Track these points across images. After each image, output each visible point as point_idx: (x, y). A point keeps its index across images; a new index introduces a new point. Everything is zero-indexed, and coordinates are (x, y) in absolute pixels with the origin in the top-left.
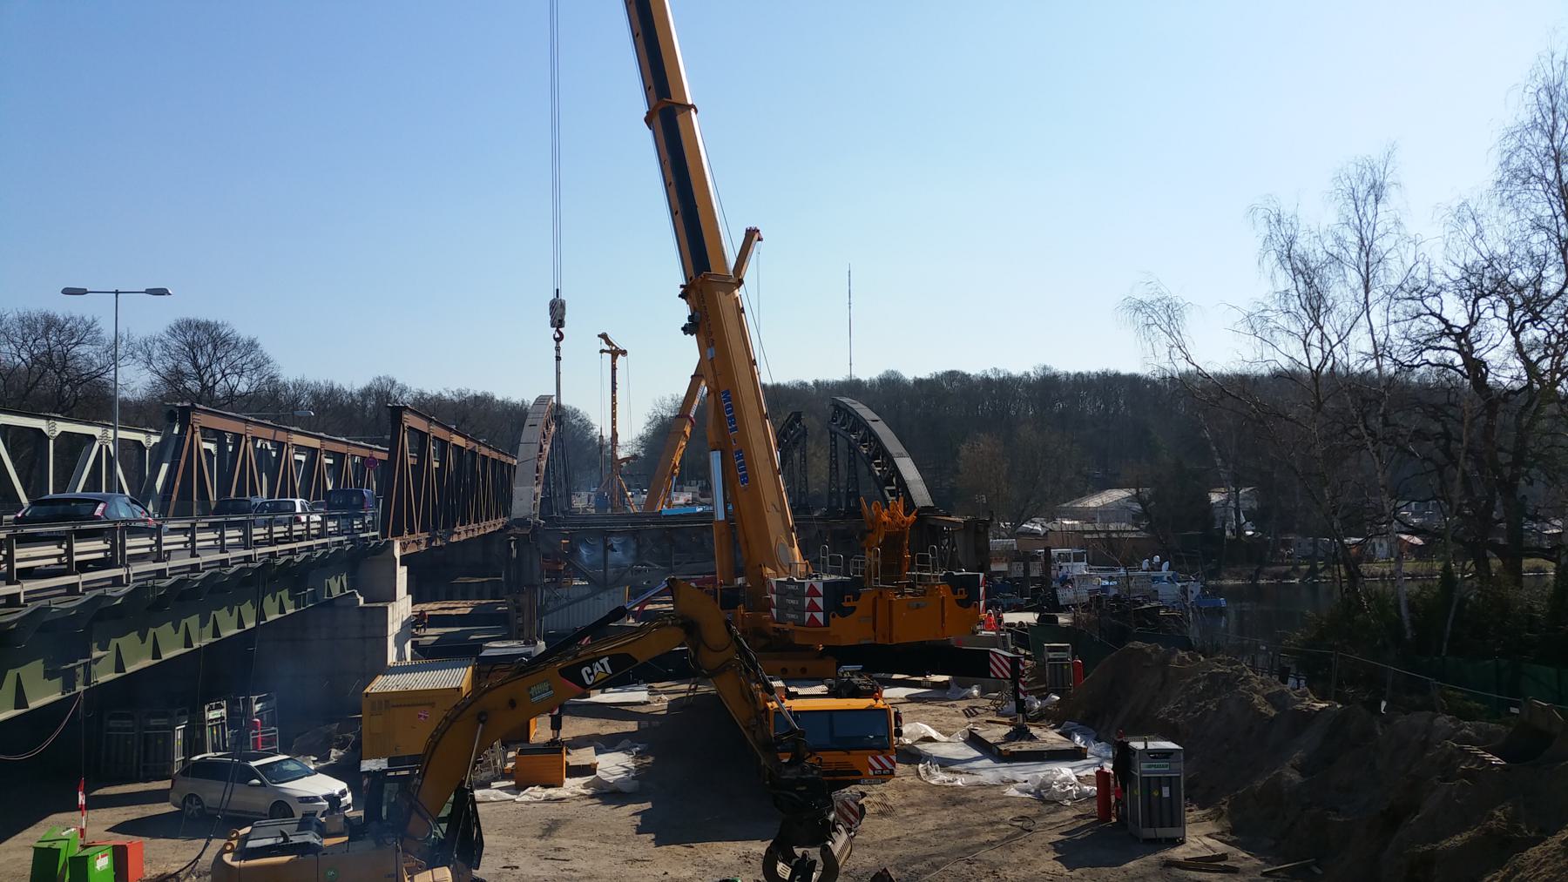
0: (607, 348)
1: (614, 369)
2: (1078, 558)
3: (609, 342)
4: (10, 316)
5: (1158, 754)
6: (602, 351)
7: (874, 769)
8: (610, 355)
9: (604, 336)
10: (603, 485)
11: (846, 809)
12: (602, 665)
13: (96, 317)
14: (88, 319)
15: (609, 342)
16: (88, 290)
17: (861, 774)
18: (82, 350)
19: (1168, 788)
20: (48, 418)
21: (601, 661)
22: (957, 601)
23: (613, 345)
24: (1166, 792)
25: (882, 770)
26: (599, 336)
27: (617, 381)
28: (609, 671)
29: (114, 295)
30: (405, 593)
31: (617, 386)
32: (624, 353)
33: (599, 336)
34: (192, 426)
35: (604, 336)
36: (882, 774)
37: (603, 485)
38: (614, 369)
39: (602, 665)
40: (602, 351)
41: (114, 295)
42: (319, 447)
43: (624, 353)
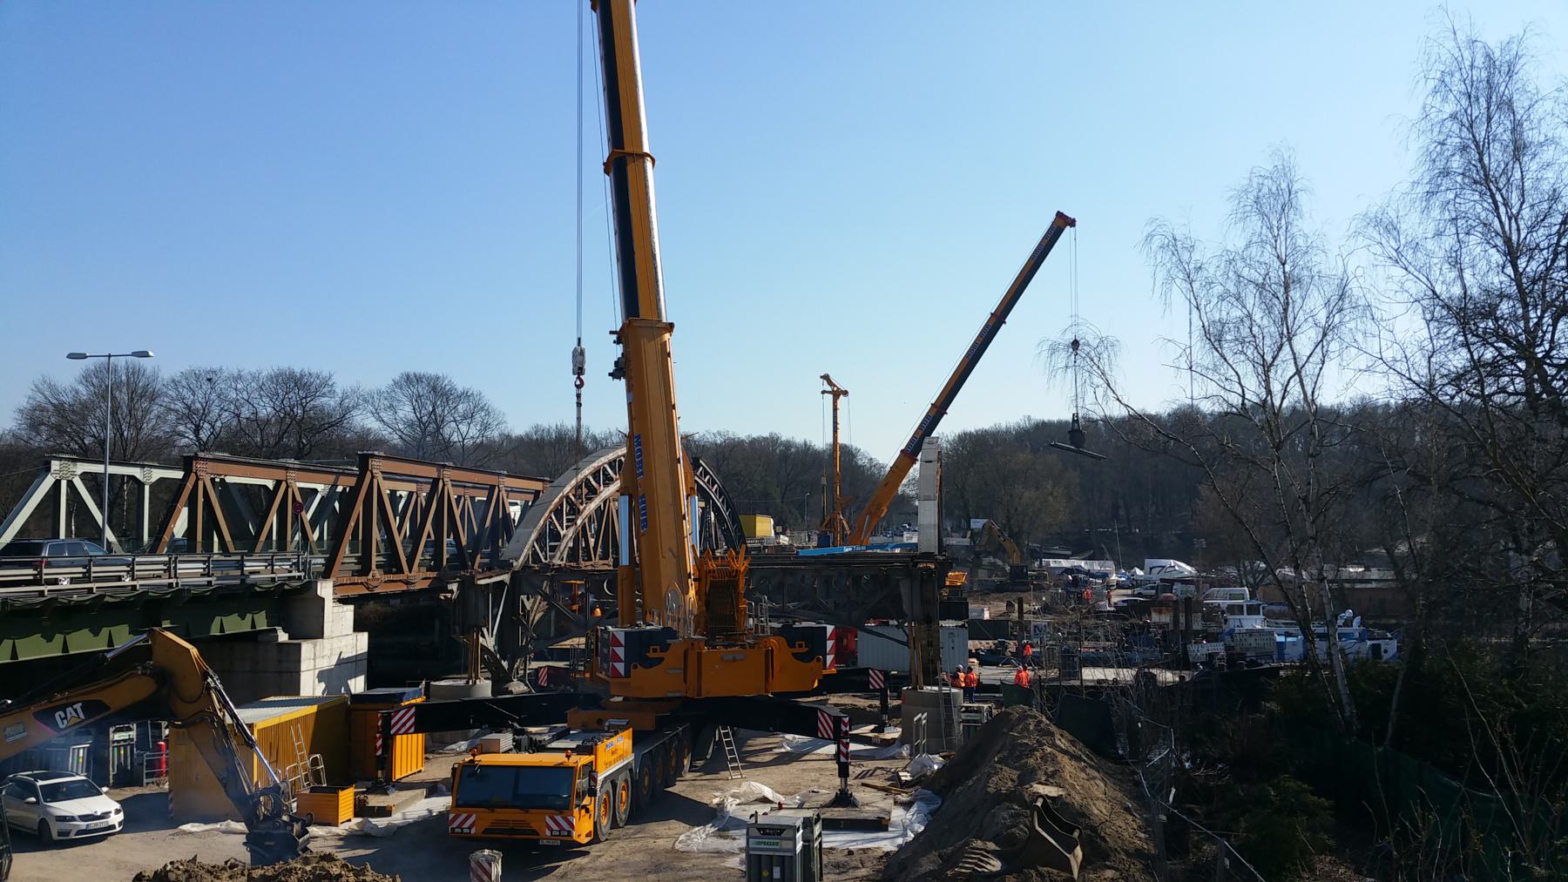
0: (829, 388)
1: (835, 409)
2: (1253, 610)
3: (830, 383)
4: (265, 373)
5: (770, 829)
6: (823, 392)
7: (552, 830)
8: (831, 396)
9: (826, 377)
10: (825, 524)
11: (479, 869)
12: (75, 710)
13: (332, 373)
14: (325, 374)
15: (830, 383)
16: (88, 354)
17: (538, 835)
18: (318, 402)
19: (778, 868)
20: (143, 466)
21: (75, 706)
22: (793, 654)
23: (835, 386)
24: (777, 874)
25: (560, 831)
26: (821, 377)
27: (838, 422)
28: (82, 716)
29: (107, 358)
30: (352, 630)
31: (838, 426)
32: (845, 393)
33: (821, 377)
34: (371, 472)
35: (826, 377)
36: (560, 835)
37: (825, 524)
38: (835, 409)
39: (75, 710)
40: (823, 392)
41: (107, 358)
42: (541, 489)
43: (845, 393)
